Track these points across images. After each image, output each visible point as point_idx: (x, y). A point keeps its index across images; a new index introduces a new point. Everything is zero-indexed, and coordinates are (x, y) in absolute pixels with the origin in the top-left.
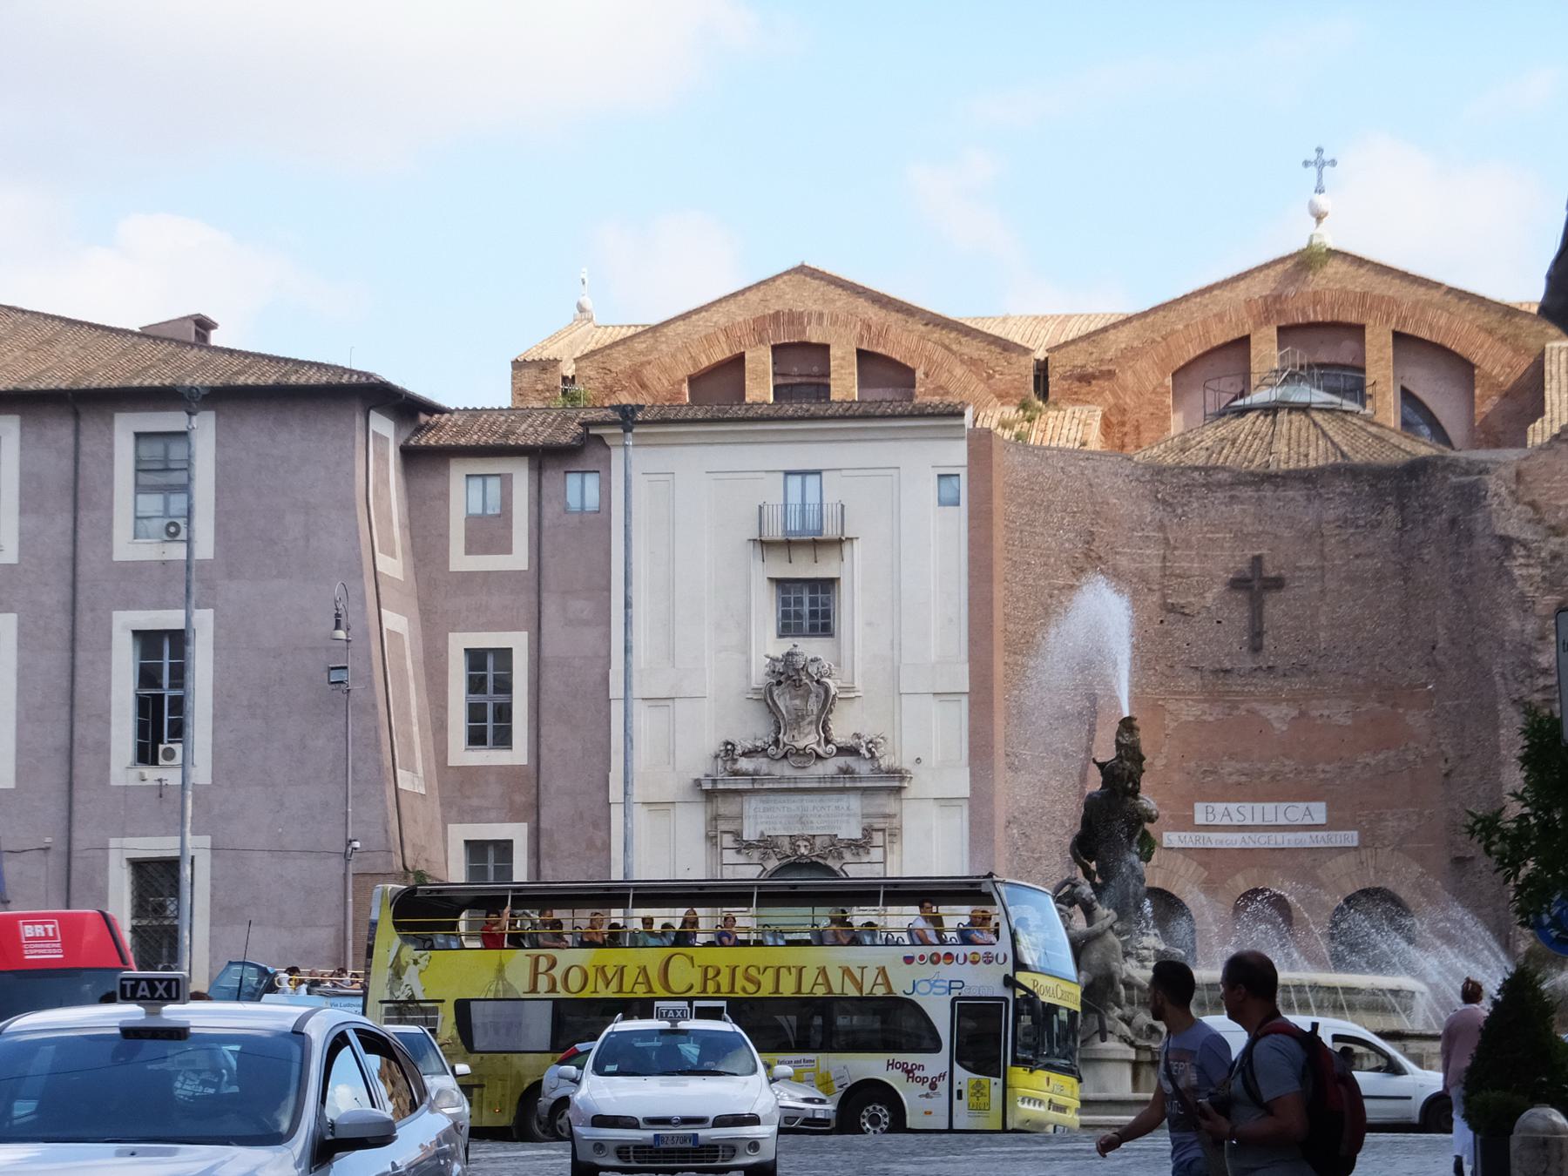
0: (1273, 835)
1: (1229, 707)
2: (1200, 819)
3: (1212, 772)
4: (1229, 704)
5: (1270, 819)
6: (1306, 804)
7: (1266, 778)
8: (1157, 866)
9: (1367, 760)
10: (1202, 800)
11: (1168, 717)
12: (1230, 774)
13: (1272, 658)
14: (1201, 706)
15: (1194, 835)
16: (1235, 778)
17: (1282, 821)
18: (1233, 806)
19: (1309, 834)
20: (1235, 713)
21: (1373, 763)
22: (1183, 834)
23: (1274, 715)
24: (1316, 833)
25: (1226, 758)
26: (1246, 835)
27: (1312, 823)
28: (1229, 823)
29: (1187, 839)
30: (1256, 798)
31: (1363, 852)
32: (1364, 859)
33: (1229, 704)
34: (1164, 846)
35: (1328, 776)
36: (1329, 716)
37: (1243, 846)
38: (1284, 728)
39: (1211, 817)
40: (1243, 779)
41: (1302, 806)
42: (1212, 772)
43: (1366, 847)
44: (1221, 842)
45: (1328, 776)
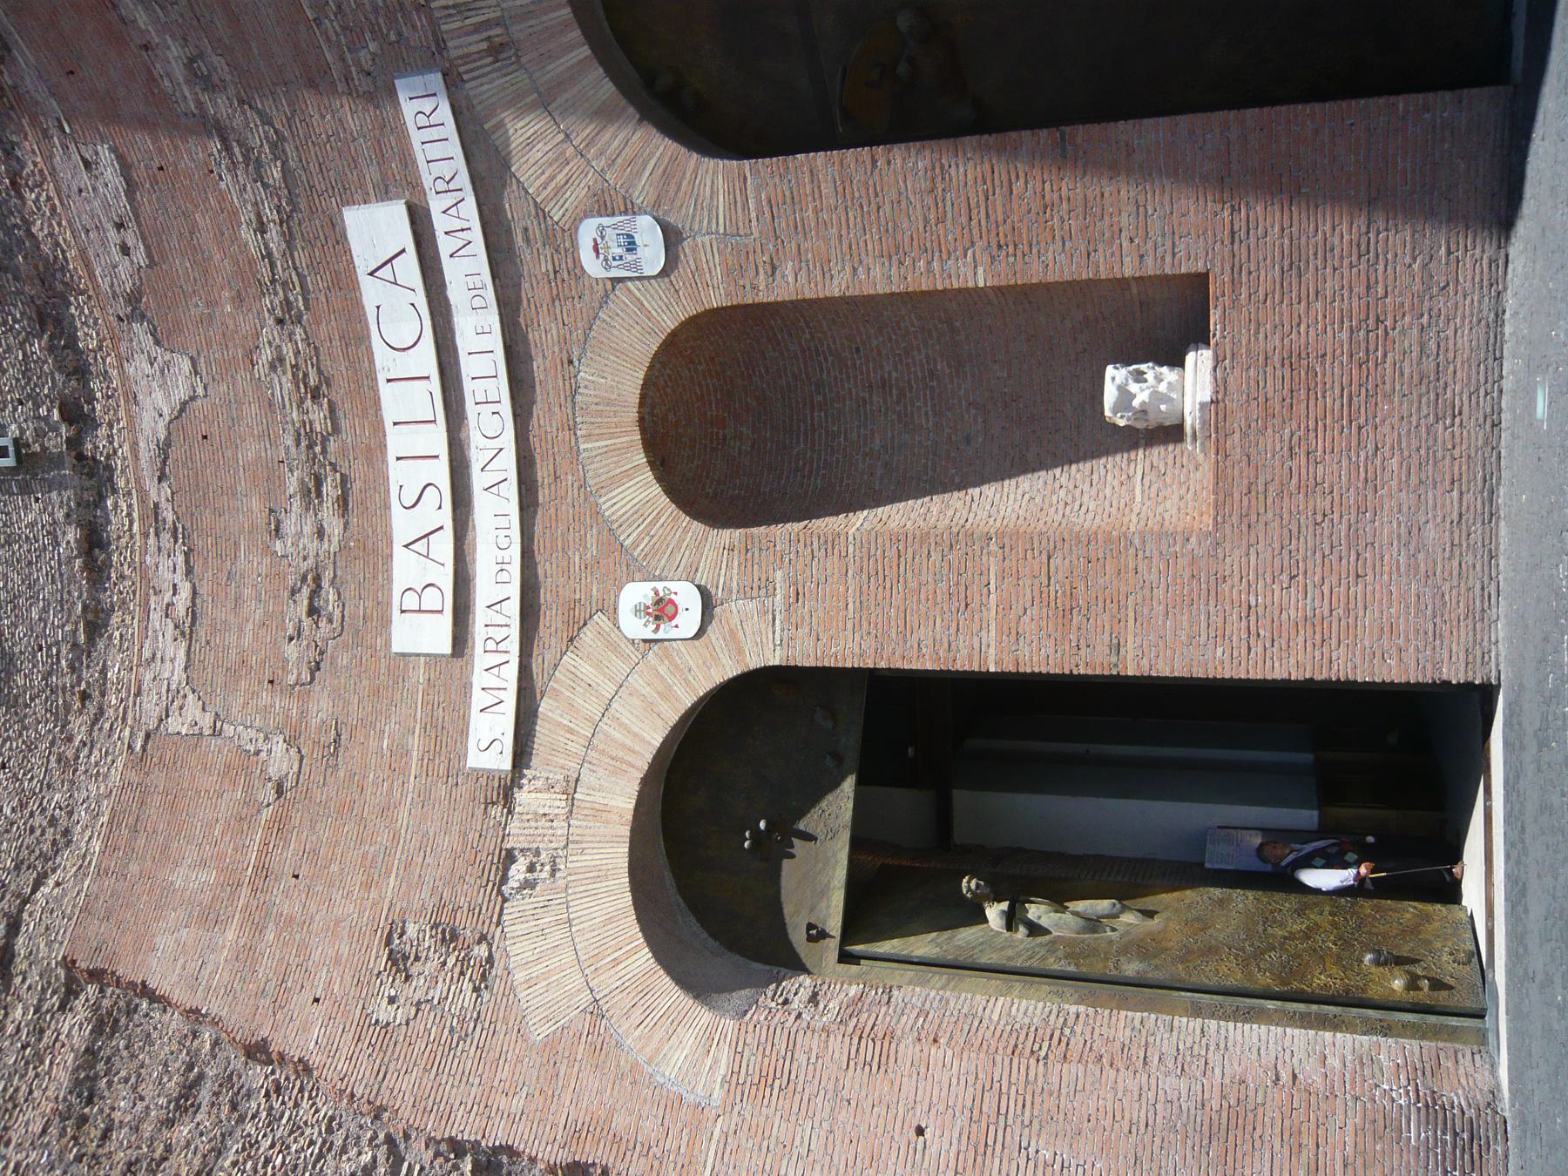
0: (472, 390)
1: (157, 535)
2: (435, 636)
3: (316, 592)
4: (152, 540)
5: (425, 399)
6: (365, 282)
7: (318, 416)
8: (571, 787)
9: (179, 73)
10: (386, 622)
11: (175, 724)
12: (320, 533)
13: (43, 411)
14: (156, 617)
15: (481, 659)
16: (329, 516)
17: (425, 359)
18: (403, 525)
19: (447, 264)
20: (169, 516)
21: (174, 51)
22: (479, 699)
23: (158, 395)
24: (440, 234)
25: (278, 546)
26: (479, 480)
27: (411, 256)
28: (447, 536)
29: (495, 683)
30: (376, 450)
31: (455, 48)
32: (476, 44)
33: (152, 540)
34: (507, 765)
35: (269, 213)
36: (120, 226)
37: (511, 490)
38: (186, 365)
39: (431, 599)
40: (330, 489)
41: (371, 292)
42: (316, 592)
43: (440, 44)
44: (502, 566)
45: (269, 213)
